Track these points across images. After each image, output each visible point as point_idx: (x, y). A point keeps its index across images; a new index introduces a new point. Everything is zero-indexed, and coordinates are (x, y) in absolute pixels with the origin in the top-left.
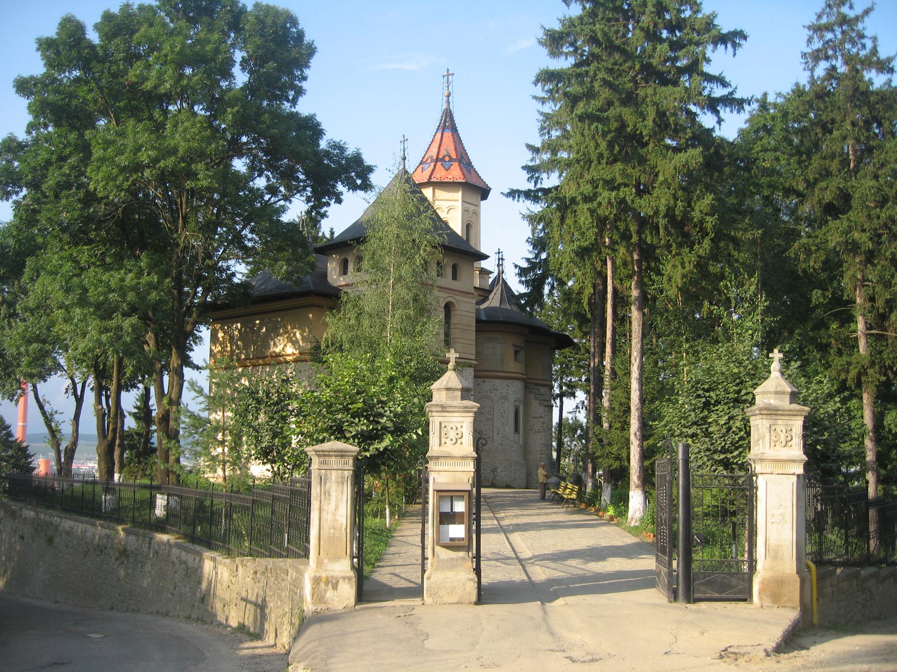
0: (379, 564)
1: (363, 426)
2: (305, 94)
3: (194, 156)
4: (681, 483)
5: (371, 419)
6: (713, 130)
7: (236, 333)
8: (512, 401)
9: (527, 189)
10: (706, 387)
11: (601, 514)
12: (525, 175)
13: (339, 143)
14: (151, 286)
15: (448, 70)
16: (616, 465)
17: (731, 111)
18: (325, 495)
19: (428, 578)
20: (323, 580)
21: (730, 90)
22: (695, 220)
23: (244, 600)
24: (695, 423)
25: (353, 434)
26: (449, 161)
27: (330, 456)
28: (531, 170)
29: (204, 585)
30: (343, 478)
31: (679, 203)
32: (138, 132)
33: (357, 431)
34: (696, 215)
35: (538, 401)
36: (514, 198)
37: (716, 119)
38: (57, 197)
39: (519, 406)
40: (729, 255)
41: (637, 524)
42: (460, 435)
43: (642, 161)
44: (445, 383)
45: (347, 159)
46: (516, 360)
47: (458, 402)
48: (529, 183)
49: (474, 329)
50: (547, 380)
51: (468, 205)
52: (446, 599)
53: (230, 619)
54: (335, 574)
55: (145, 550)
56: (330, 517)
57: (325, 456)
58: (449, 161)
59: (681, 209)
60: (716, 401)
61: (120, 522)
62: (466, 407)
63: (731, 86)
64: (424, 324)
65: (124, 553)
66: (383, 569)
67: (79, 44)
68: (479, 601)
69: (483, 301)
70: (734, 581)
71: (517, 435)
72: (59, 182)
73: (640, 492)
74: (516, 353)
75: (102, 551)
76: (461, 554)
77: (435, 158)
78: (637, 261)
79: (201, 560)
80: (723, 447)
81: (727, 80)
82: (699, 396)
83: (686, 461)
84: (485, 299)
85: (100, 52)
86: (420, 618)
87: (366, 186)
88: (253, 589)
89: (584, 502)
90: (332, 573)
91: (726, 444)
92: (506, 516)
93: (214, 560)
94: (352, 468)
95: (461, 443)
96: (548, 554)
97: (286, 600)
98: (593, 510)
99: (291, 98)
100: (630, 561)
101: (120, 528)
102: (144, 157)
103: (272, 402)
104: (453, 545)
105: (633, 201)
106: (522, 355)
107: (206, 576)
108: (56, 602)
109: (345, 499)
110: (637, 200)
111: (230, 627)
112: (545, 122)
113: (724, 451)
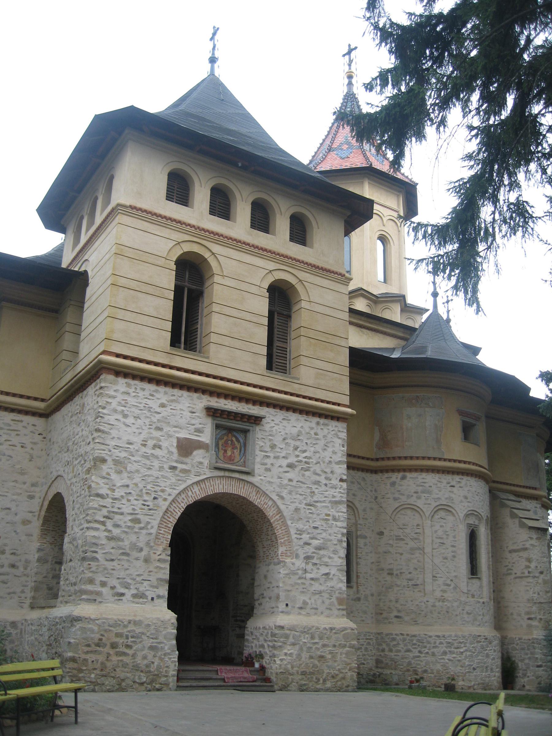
8: (462, 515)
15: (349, 45)
35: (517, 521)
39: (476, 526)
71: (476, 582)
106: (480, 430)
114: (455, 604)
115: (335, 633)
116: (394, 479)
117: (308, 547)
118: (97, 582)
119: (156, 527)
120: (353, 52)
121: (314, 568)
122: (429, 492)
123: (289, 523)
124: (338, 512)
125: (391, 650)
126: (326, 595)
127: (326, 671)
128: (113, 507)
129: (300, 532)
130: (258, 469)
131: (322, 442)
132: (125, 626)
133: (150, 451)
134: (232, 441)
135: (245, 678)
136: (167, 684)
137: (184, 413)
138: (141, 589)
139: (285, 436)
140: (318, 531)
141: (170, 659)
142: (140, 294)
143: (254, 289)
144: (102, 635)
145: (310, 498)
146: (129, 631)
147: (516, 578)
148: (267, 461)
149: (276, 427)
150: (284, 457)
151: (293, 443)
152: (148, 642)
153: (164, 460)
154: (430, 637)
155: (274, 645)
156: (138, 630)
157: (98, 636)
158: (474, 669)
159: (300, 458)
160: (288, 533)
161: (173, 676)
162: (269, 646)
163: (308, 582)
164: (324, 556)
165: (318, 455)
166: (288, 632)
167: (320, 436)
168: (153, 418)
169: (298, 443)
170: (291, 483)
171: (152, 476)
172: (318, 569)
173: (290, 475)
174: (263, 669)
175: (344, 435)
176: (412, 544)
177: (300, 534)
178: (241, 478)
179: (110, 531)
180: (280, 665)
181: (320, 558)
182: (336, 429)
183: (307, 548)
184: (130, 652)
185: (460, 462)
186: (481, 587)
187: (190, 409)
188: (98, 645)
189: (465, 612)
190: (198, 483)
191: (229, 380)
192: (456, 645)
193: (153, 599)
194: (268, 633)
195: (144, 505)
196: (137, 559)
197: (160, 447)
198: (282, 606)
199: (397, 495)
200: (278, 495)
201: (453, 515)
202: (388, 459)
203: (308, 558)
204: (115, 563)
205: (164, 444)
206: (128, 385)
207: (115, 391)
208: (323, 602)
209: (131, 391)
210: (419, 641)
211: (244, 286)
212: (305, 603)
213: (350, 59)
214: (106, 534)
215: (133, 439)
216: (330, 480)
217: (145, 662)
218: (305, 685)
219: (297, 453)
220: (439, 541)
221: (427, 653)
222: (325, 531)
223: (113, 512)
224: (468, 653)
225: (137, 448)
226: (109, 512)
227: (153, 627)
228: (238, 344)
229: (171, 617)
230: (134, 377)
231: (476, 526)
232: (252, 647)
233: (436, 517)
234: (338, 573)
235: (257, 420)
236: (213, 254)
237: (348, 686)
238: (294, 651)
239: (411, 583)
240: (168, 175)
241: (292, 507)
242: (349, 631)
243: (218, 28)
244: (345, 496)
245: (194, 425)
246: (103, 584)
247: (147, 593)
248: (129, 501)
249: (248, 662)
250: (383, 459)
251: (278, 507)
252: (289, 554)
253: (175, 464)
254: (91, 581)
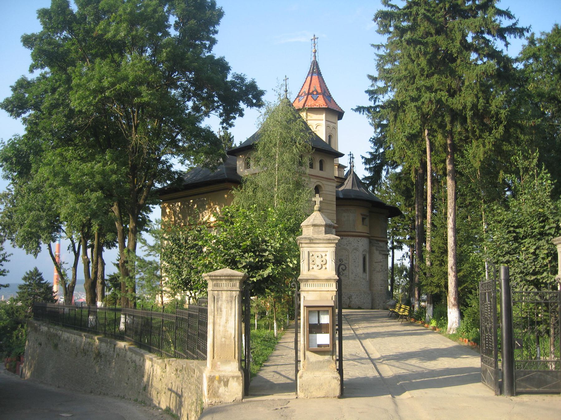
0: (265, 364)
1: (249, 258)
2: (217, 43)
3: (139, 82)
4: (503, 298)
5: (257, 254)
6: (501, 52)
7: (178, 209)
9: (369, 106)
10: (516, 224)
11: (426, 325)
12: (367, 96)
13: (240, 75)
14: (114, 172)
15: (314, 36)
16: (437, 291)
17: (515, 37)
18: (218, 311)
19: (301, 377)
20: (217, 379)
21: (514, 21)
22: (492, 112)
23: (170, 390)
24: (508, 253)
25: (243, 265)
26: (316, 94)
27: (221, 280)
28: (372, 93)
29: (145, 379)
30: (231, 297)
31: (481, 100)
32: (102, 67)
33: (246, 262)
34: (493, 108)
35: (378, 252)
36: (360, 112)
37: (504, 43)
38: (50, 114)
39: (366, 255)
40: (517, 137)
41: (454, 332)
42: (324, 262)
43: (453, 73)
44: (312, 220)
45: (246, 85)
46: (363, 224)
47: (323, 236)
48: (370, 102)
49: (335, 203)
50: (384, 238)
51: (329, 123)
52: (315, 394)
53: (161, 403)
54: (226, 374)
55: (111, 352)
56: (221, 328)
57: (217, 280)
58: (316, 94)
59: (483, 104)
60: (523, 236)
61: (97, 333)
62: (329, 240)
63: (515, 18)
64: (300, 194)
65: (99, 355)
66: (268, 368)
67: (64, 12)
68: (342, 395)
69: (341, 186)
70: (549, 377)
72: (52, 104)
73: (456, 309)
74: (363, 219)
75: (85, 353)
76: (327, 357)
77: (307, 92)
78: (450, 144)
79: (144, 360)
80: (534, 270)
81: (512, 13)
82: (509, 232)
83: (508, 281)
84: (342, 184)
85: (78, 17)
86: (293, 411)
87: (259, 104)
88: (175, 382)
89: (413, 318)
90: (223, 373)
91: (536, 268)
92: (359, 328)
93: (151, 360)
94: (239, 289)
95: (326, 268)
96: (393, 355)
97: (193, 392)
98: (420, 323)
99: (207, 46)
100: (455, 360)
101: (96, 338)
102: (106, 84)
103: (189, 246)
104: (321, 350)
105: (447, 100)
106: (367, 221)
107: (147, 371)
108: (59, 387)
109: (233, 314)
110: (450, 99)
111: (161, 409)
112: (380, 61)
113: (535, 273)
122: (351, 244)
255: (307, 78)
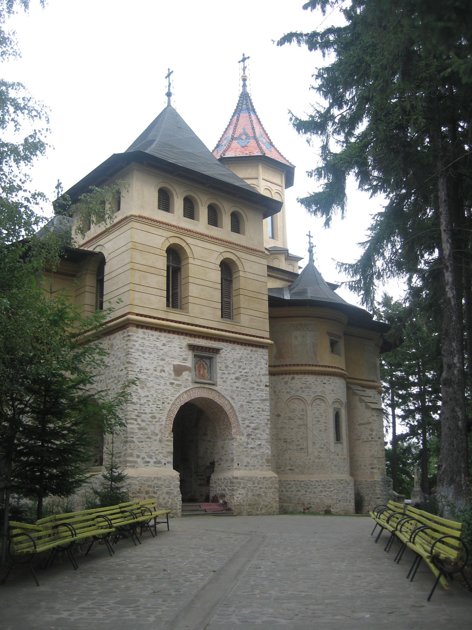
8: (330, 403)
15: (244, 55)
35: (364, 404)
39: (339, 409)
51: (269, 184)
71: (339, 445)
74: (333, 344)
106: (341, 345)
114: (327, 460)
115: (266, 480)
116: (286, 379)
117: (249, 428)
118: (135, 455)
119: (165, 420)
120: (247, 60)
121: (253, 441)
123: (238, 414)
124: (265, 406)
125: (287, 491)
126: (259, 457)
127: (262, 503)
128: (140, 410)
129: (244, 419)
130: (219, 381)
131: (254, 363)
132: (152, 481)
133: (159, 374)
134: (203, 364)
135: (217, 509)
136: (176, 514)
137: (176, 349)
138: (158, 459)
139: (233, 360)
140: (254, 418)
141: (177, 499)
142: (147, 274)
143: (212, 266)
144: (141, 487)
145: (248, 398)
146: (155, 484)
147: (363, 442)
148: (224, 376)
149: (228, 354)
150: (233, 373)
151: (238, 364)
152: (165, 490)
153: (167, 379)
154: (312, 481)
155: (233, 489)
156: (160, 483)
157: (138, 487)
158: (339, 501)
159: (242, 373)
160: (237, 420)
161: (180, 509)
162: (229, 489)
163: (249, 450)
164: (258, 433)
165: (252, 371)
166: (240, 481)
167: (253, 359)
168: (159, 353)
169: (241, 364)
170: (238, 389)
171: (161, 389)
172: (255, 442)
173: (237, 384)
174: (225, 503)
175: (266, 357)
176: (300, 422)
177: (244, 421)
178: (210, 387)
179: (139, 424)
180: (237, 501)
181: (256, 435)
182: (262, 354)
183: (248, 429)
184: (156, 496)
185: (329, 367)
186: (342, 448)
187: (179, 346)
188: (139, 493)
189: (333, 465)
190: (186, 392)
191: (200, 326)
192: (328, 486)
193: (165, 464)
194: (228, 482)
195: (157, 407)
196: (155, 440)
197: (164, 371)
198: (235, 465)
199: (289, 390)
200: (230, 397)
201: (325, 402)
202: (283, 366)
203: (249, 435)
204: (144, 443)
205: (166, 369)
206: (144, 333)
207: (137, 337)
208: (258, 462)
209: (146, 337)
210: (305, 484)
211: (206, 264)
212: (248, 463)
213: (244, 64)
214: (138, 426)
215: (149, 367)
216: (260, 386)
217: (164, 501)
218: (250, 512)
219: (240, 370)
220: (316, 419)
221: (311, 492)
222: (258, 418)
223: (141, 413)
224: (336, 491)
225: (151, 372)
226: (139, 413)
227: (167, 481)
228: (204, 302)
229: (176, 474)
230: (147, 328)
231: (339, 409)
232: (216, 491)
233: (314, 404)
234: (266, 444)
235: (217, 351)
236: (187, 244)
237: (274, 512)
238: (243, 491)
239: (299, 447)
240: (159, 192)
241: (239, 404)
242: (274, 479)
243: (172, 72)
244: (268, 395)
245: (182, 356)
246: (138, 456)
247: (162, 461)
248: (149, 405)
249: (215, 500)
250: (279, 366)
251: (231, 404)
252: (238, 433)
253: (173, 381)
254: (131, 455)
255: (231, 120)
